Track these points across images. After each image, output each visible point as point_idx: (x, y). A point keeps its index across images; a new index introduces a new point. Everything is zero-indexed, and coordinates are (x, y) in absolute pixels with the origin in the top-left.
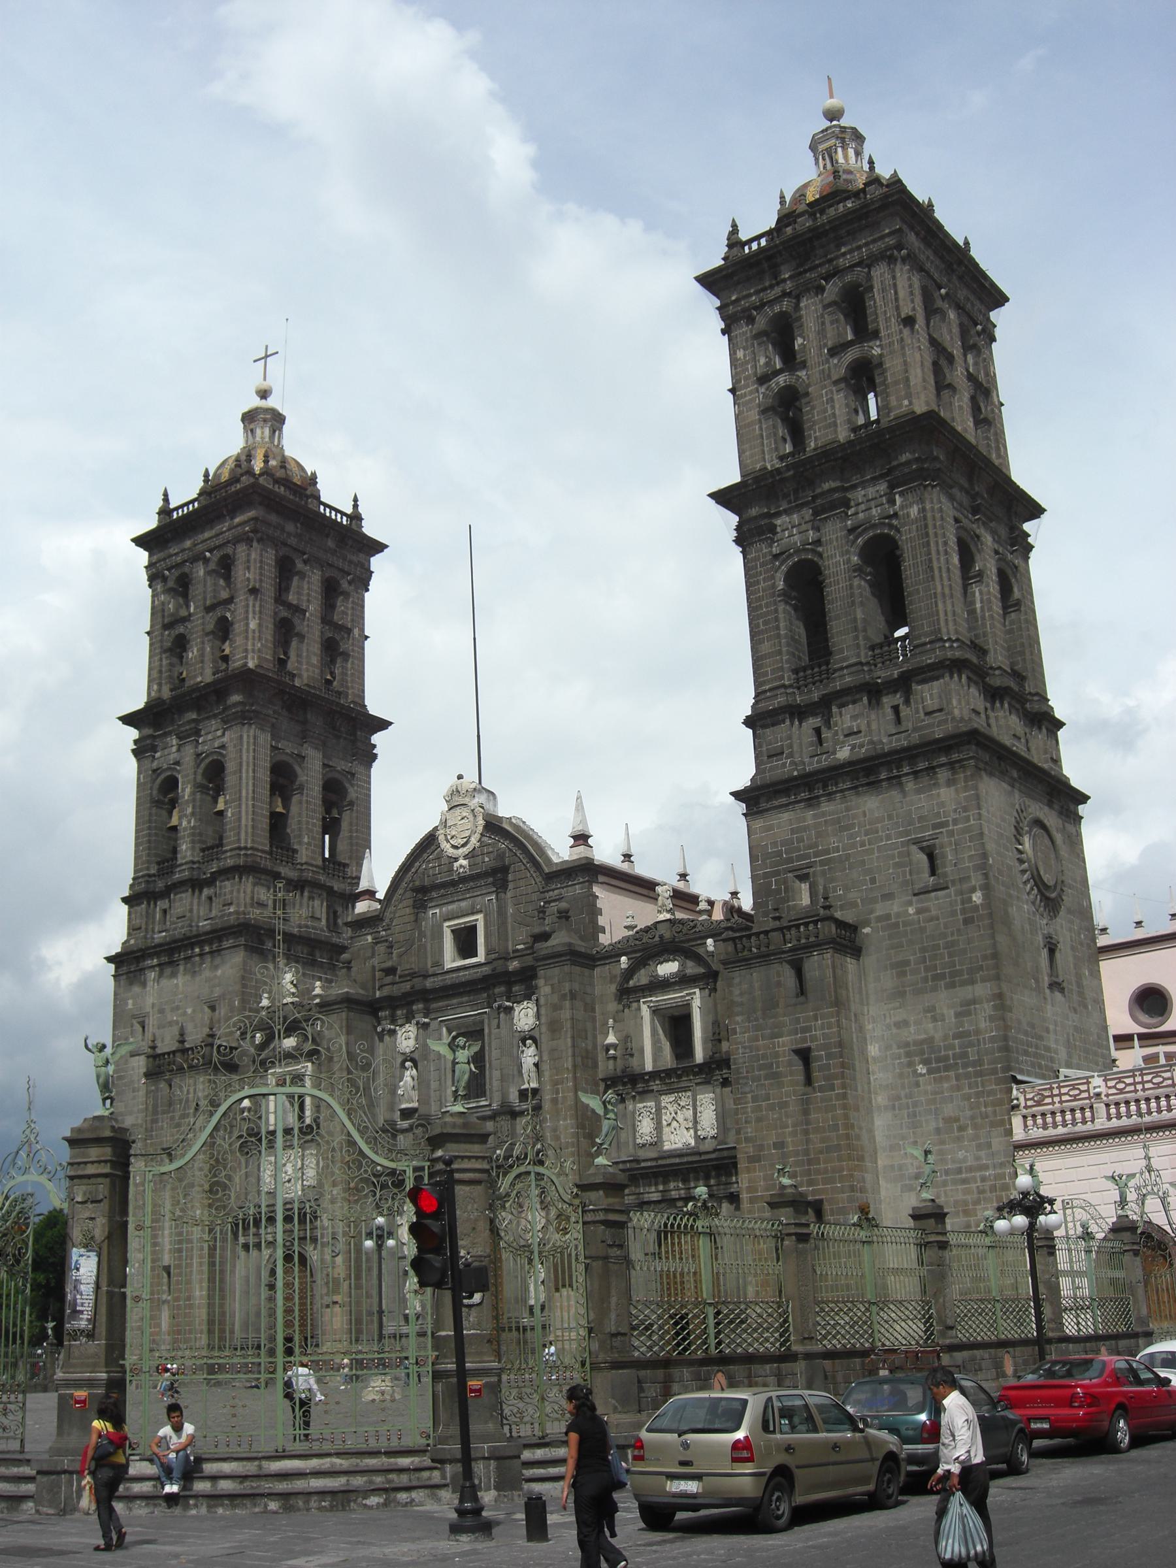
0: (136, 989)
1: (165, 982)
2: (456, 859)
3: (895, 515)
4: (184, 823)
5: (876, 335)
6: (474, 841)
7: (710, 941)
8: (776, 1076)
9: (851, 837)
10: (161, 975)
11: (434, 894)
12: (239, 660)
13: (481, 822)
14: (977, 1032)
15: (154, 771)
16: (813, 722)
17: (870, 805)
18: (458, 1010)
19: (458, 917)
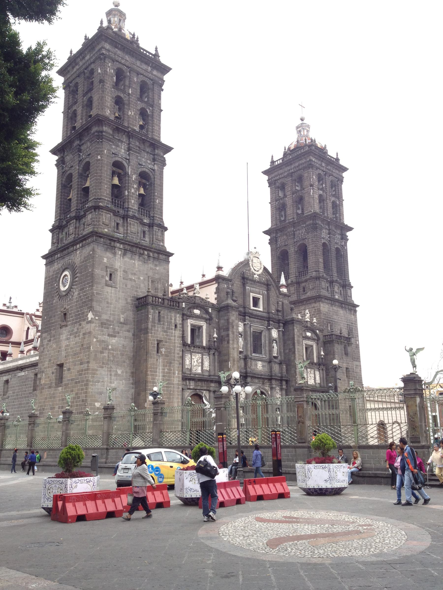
0: (109, 254)
1: (126, 259)
2: (255, 274)
3: (342, 246)
4: (133, 191)
5: (339, 199)
6: (261, 271)
7: (318, 331)
8: (343, 373)
9: (338, 318)
10: (124, 254)
11: (248, 281)
12: (156, 136)
13: (263, 267)
14: (358, 373)
15: (113, 153)
16: (328, 285)
17: (341, 312)
18: (257, 324)
19: (255, 293)
